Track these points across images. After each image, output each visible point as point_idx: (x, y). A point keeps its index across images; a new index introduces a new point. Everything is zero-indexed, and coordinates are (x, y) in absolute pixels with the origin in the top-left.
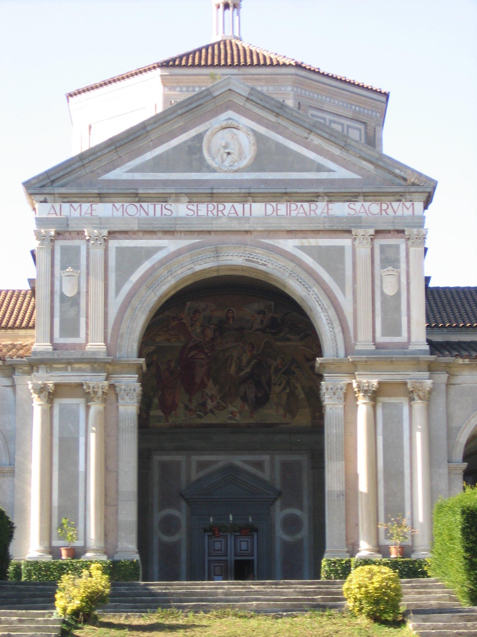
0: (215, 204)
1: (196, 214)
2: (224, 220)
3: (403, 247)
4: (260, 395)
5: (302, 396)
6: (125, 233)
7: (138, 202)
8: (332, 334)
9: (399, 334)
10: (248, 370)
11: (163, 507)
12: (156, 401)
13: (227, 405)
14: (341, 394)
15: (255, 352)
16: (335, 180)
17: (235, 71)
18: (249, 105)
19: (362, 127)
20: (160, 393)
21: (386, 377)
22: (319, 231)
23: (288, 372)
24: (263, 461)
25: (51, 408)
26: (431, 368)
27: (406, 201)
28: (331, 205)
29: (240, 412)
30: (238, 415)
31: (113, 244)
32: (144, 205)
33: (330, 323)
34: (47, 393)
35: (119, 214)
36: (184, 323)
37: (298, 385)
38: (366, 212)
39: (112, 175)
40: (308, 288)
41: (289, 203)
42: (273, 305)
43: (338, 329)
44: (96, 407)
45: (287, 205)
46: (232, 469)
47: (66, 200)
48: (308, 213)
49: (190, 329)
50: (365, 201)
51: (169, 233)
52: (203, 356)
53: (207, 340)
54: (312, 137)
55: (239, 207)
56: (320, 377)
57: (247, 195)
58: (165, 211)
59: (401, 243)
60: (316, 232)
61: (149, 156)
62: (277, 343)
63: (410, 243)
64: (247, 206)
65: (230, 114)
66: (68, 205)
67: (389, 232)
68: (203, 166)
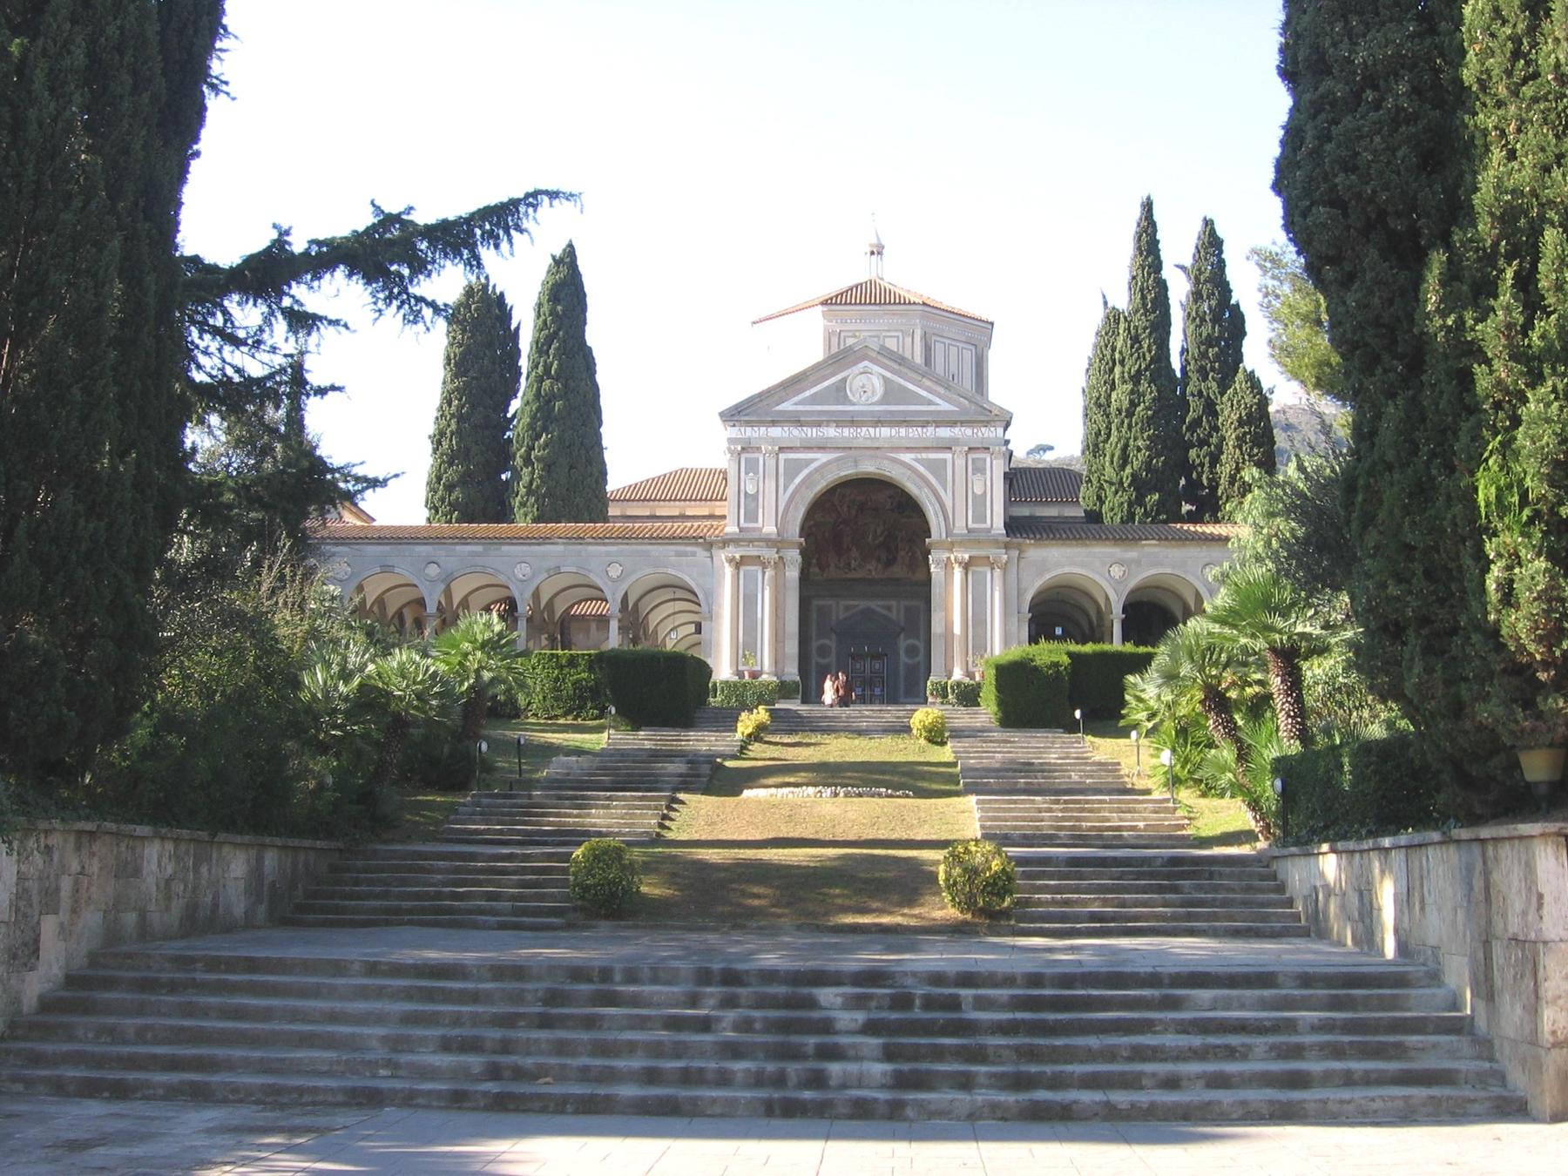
2: (861, 440)
3: (988, 460)
6: (791, 449)
9: (985, 522)
10: (881, 539)
12: (814, 561)
16: (939, 411)
17: (877, 308)
18: (879, 357)
19: (973, 348)
21: (975, 553)
25: (738, 574)
26: (1007, 547)
28: (937, 430)
31: (782, 456)
32: (805, 429)
39: (780, 408)
40: (920, 488)
43: (941, 519)
44: (769, 573)
49: (839, 509)
51: (822, 448)
54: (924, 380)
55: (872, 430)
56: (930, 553)
60: (926, 449)
61: (807, 393)
64: (878, 429)
65: (866, 363)
67: (978, 448)
68: (846, 401)
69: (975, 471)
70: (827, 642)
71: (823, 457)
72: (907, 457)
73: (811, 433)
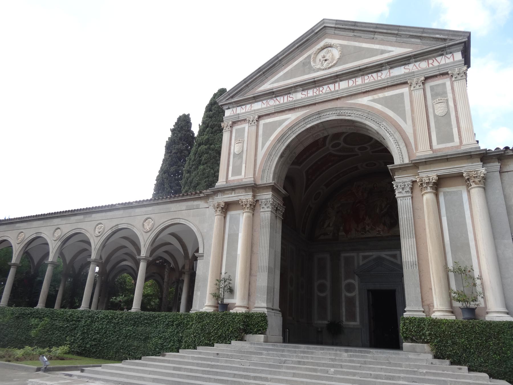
0: (318, 88)
1: (306, 96)
7: (275, 97)
8: (398, 149)
9: (452, 140)
11: (346, 279)
12: (342, 228)
14: (408, 189)
20: (343, 224)
22: (384, 88)
24: (397, 254)
25: (225, 217)
27: (447, 54)
28: (391, 71)
30: (382, 232)
32: (278, 98)
33: (397, 142)
34: (221, 208)
35: (265, 106)
38: (417, 68)
41: (363, 77)
45: (362, 77)
46: (379, 259)
47: (238, 105)
48: (376, 79)
50: (416, 62)
55: (332, 86)
57: (336, 77)
58: (289, 99)
59: (447, 81)
63: (453, 79)
64: (337, 85)
66: (240, 107)
67: (436, 76)
69: (435, 95)
70: (352, 281)
71: (292, 117)
72: (365, 100)
73: (283, 100)
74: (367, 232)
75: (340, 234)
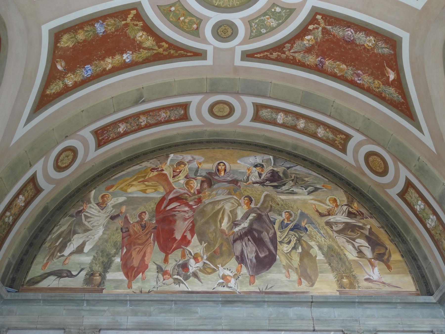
4: (262, 255)
5: (320, 257)
10: (245, 224)
12: (118, 260)
13: (218, 268)
15: (253, 206)
20: (125, 250)
23: (296, 228)
29: (236, 277)
30: (233, 280)
36: (165, 175)
37: (312, 243)
42: (272, 159)
49: (171, 180)
52: (187, 209)
53: (192, 191)
62: (280, 197)
74: (192, 278)
75: (110, 276)
